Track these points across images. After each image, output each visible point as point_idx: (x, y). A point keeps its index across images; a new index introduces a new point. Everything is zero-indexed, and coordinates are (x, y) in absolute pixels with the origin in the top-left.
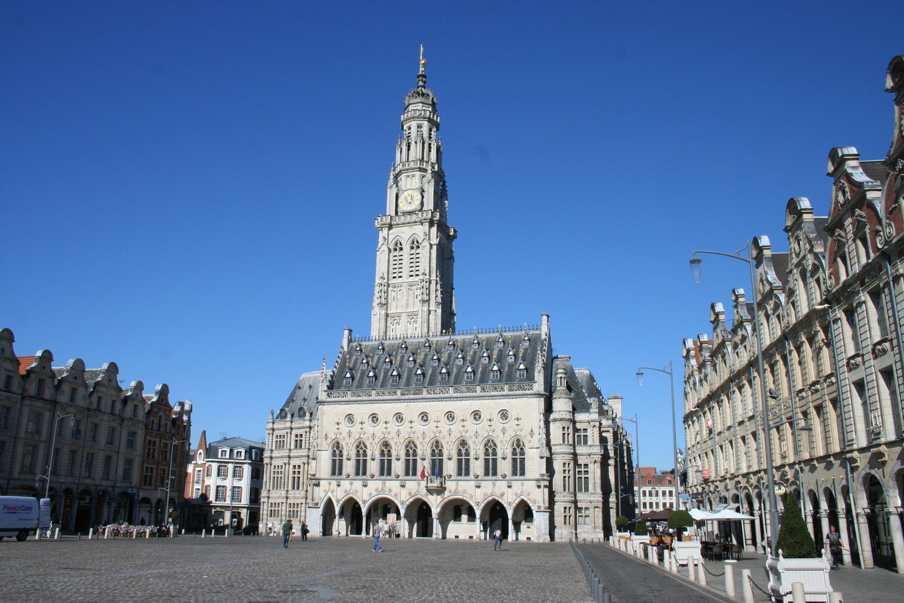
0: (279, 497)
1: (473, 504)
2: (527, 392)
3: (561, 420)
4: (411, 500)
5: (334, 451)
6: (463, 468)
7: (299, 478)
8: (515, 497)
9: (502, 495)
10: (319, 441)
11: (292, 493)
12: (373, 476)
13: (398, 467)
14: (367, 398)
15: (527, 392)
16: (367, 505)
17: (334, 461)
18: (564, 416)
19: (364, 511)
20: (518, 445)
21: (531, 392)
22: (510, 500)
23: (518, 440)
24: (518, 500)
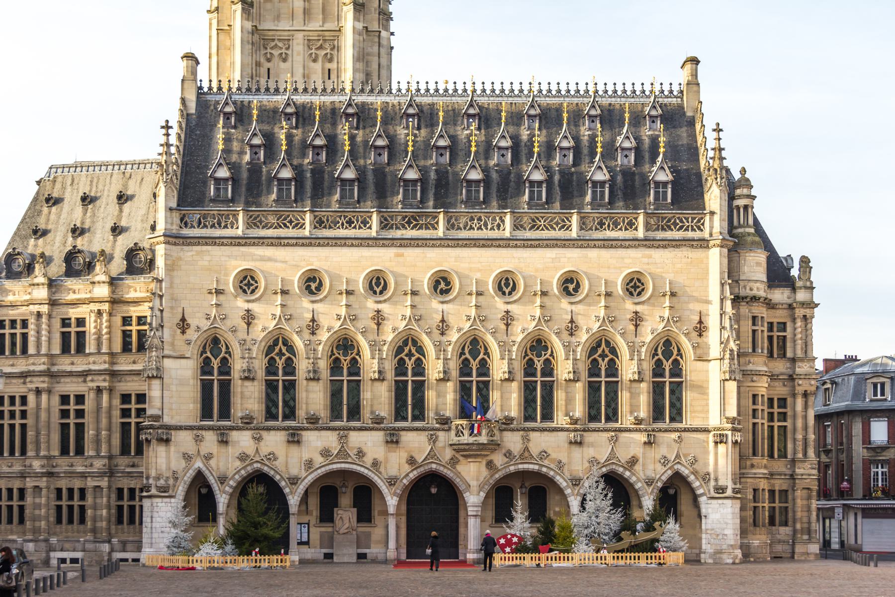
0: (23, 476)
1: (563, 484)
2: (690, 234)
3: (755, 299)
4: (412, 476)
5: (207, 361)
6: (538, 402)
7: (80, 428)
8: (660, 469)
9: (633, 461)
10: (167, 334)
11: (63, 465)
12: (313, 421)
13: (378, 398)
14: (291, 232)
15: (690, 234)
16: (301, 488)
17: (206, 388)
18: (755, 292)
19: (293, 501)
20: (667, 354)
21: (697, 234)
22: (650, 474)
23: (668, 343)
24: (670, 472)
